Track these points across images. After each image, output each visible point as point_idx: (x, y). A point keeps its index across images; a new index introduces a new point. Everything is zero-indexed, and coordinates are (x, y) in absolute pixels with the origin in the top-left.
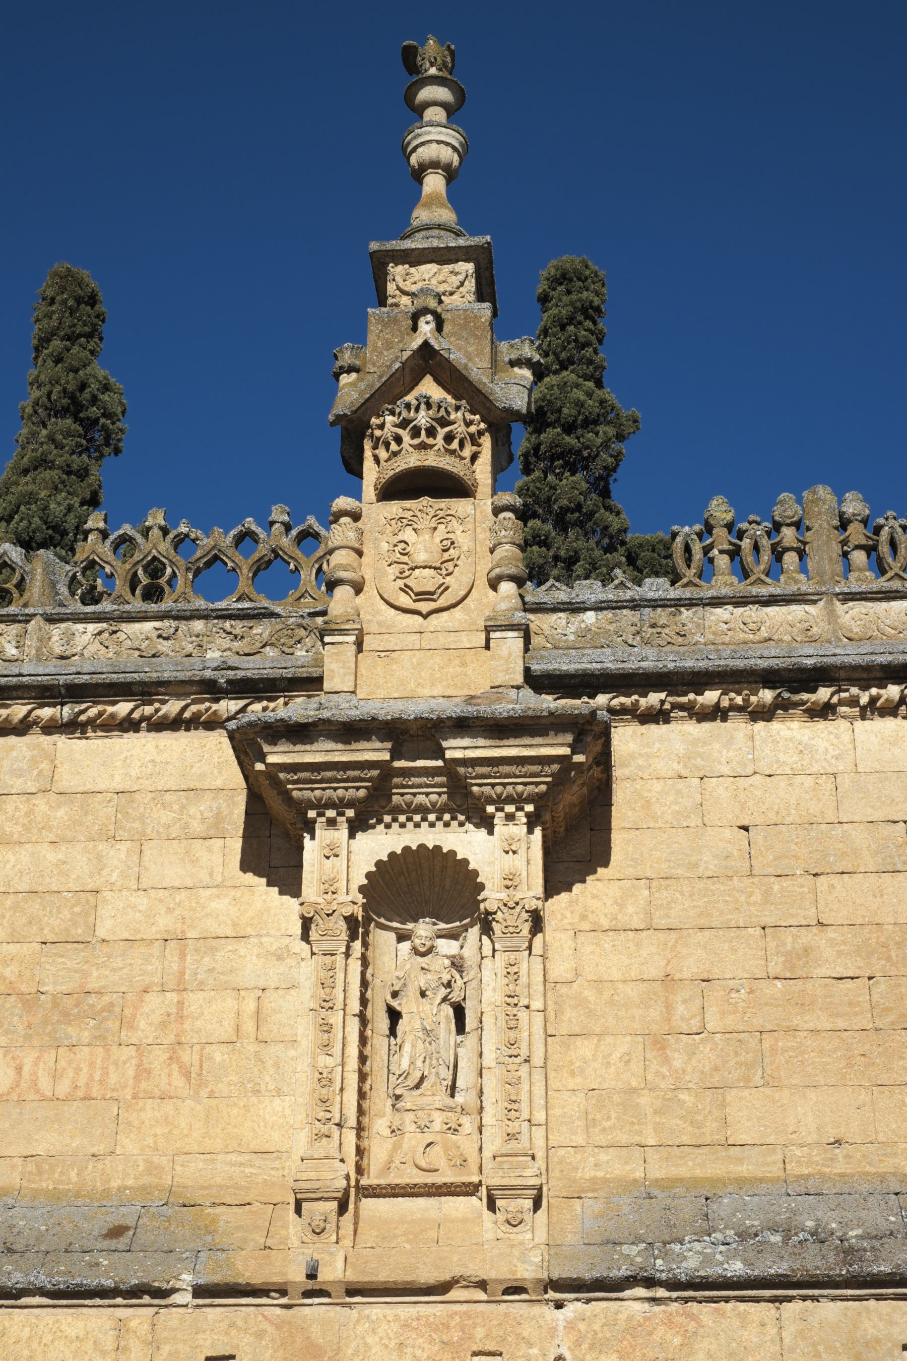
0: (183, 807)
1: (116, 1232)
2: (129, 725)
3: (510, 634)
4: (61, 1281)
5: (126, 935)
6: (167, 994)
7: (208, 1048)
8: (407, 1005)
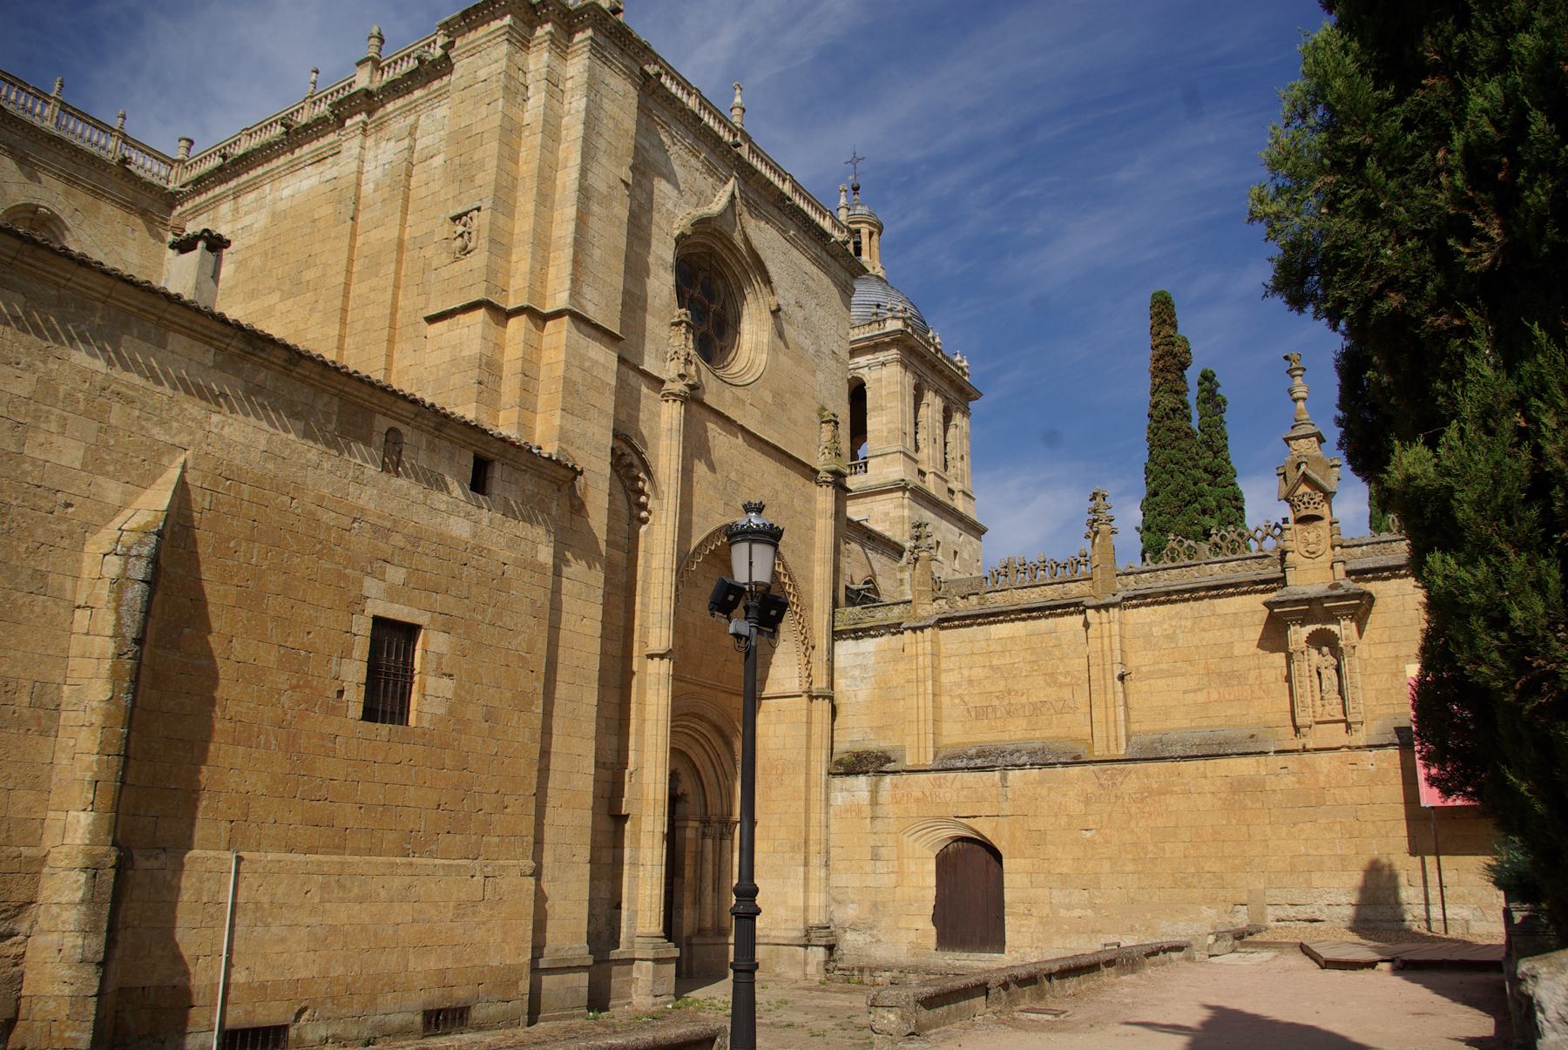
1: (1252, 736)
2: (1233, 595)
4: (1241, 752)
8: (1322, 671)
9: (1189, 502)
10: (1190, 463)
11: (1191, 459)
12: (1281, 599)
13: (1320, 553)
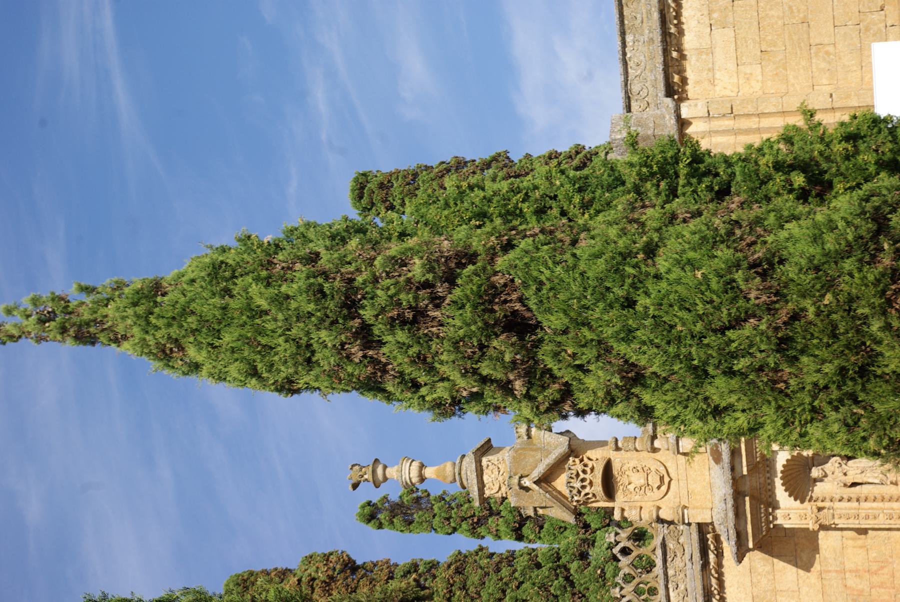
0: (759, 574)
3: (680, 444)
5: (821, 596)
6: (847, 576)
7: (870, 559)
8: (850, 480)
9: (567, 578)
10: (505, 571)
11: (498, 570)
12: (732, 532)
13: (662, 469)
